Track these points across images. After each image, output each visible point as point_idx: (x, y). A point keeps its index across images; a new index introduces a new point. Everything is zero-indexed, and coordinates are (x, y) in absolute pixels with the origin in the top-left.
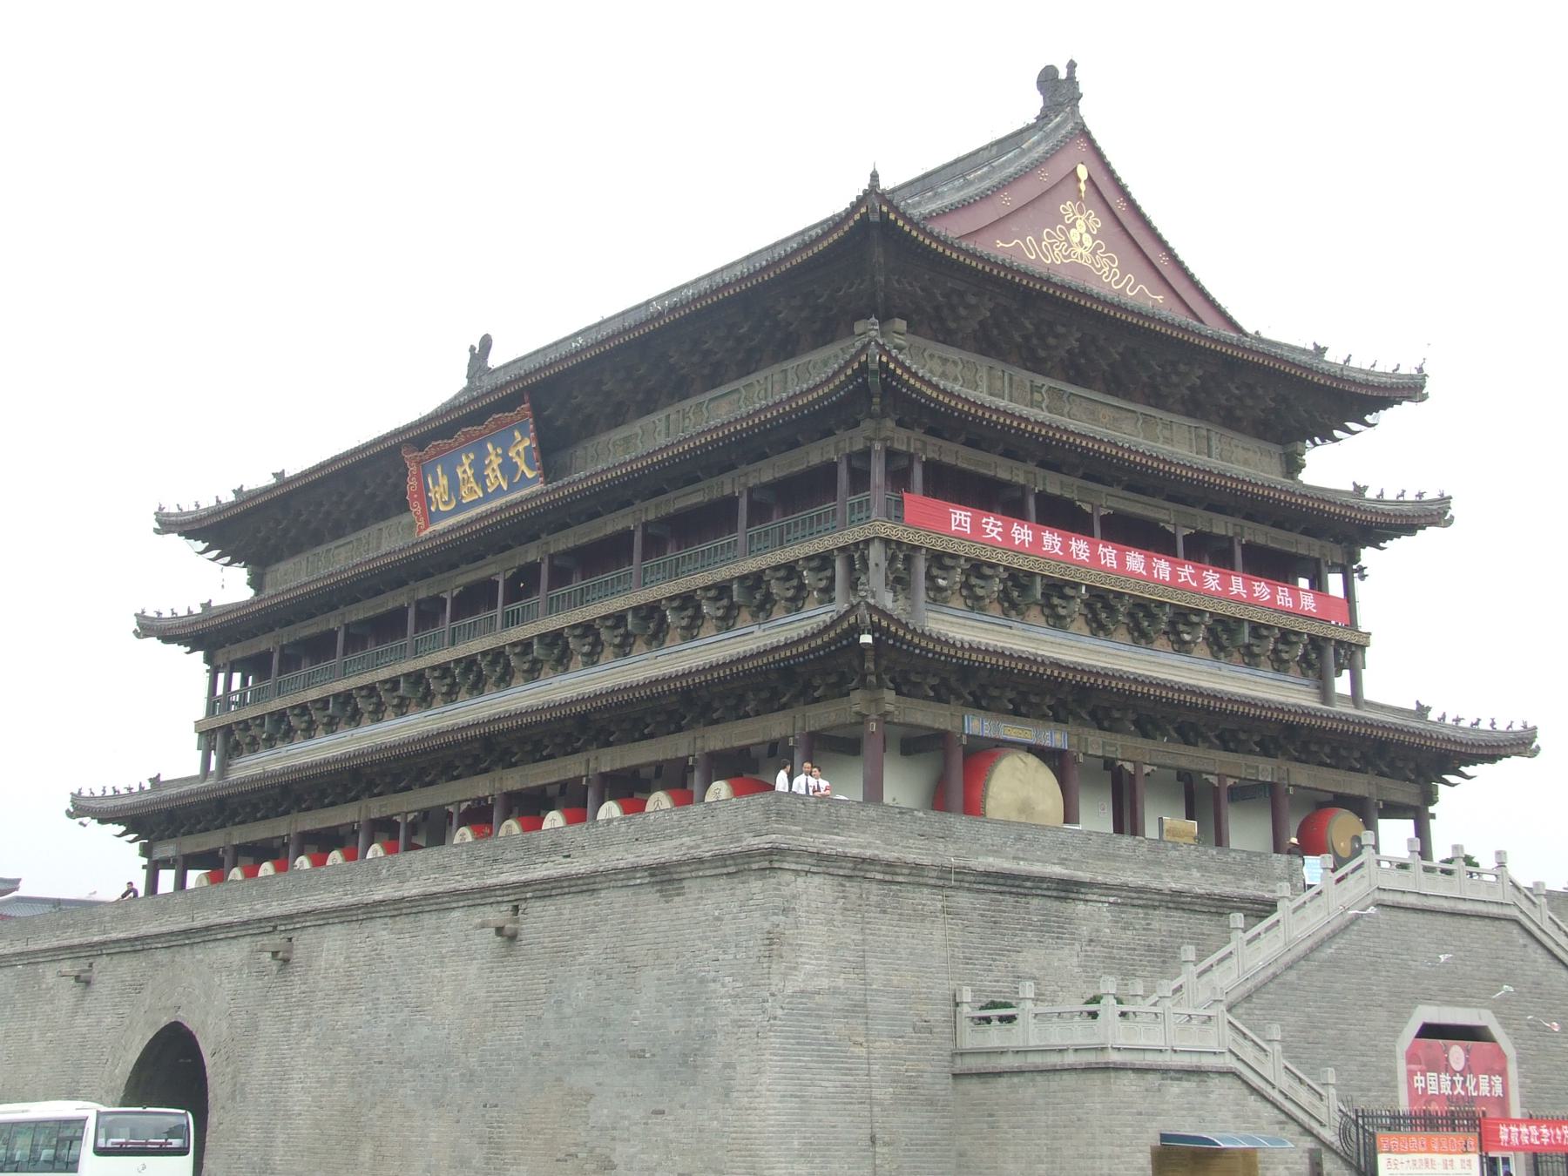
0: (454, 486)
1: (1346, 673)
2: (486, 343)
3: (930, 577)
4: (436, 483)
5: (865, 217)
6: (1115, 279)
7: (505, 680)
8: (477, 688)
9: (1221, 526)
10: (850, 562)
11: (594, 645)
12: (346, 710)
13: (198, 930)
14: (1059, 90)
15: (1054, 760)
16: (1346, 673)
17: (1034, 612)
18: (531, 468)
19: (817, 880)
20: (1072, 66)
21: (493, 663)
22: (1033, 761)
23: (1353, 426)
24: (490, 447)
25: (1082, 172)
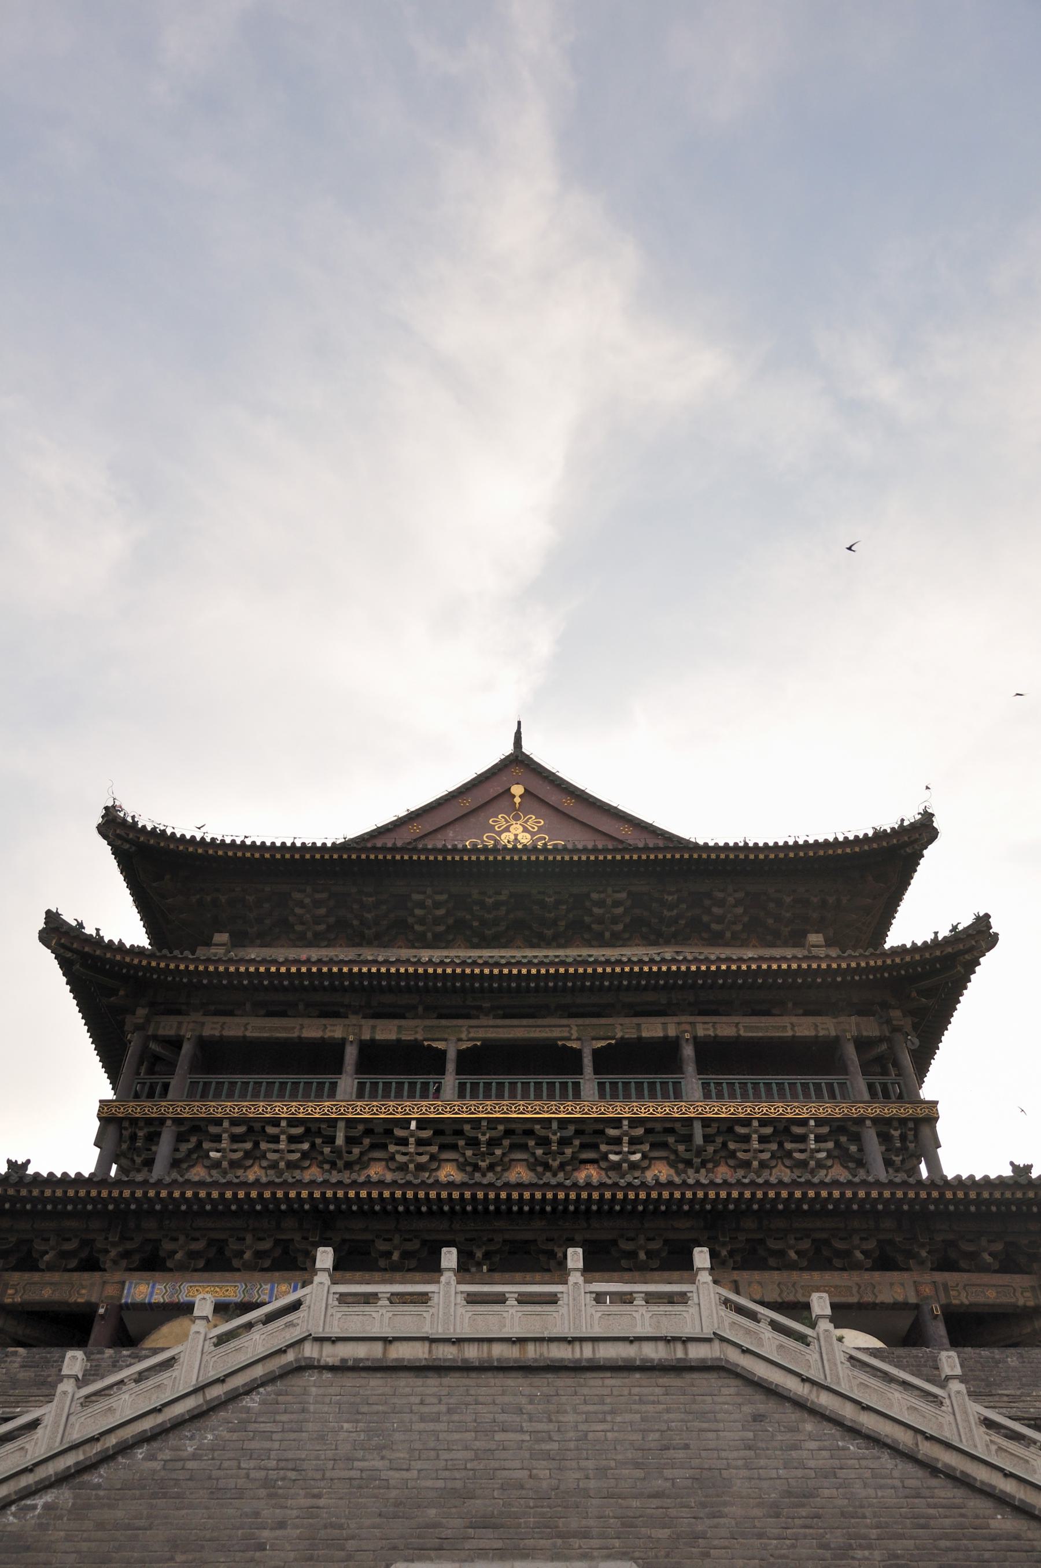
9: (653, 1029)
25: (517, 790)
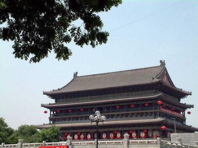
2: (77, 73)
6: (168, 84)
14: (163, 63)
20: (164, 61)
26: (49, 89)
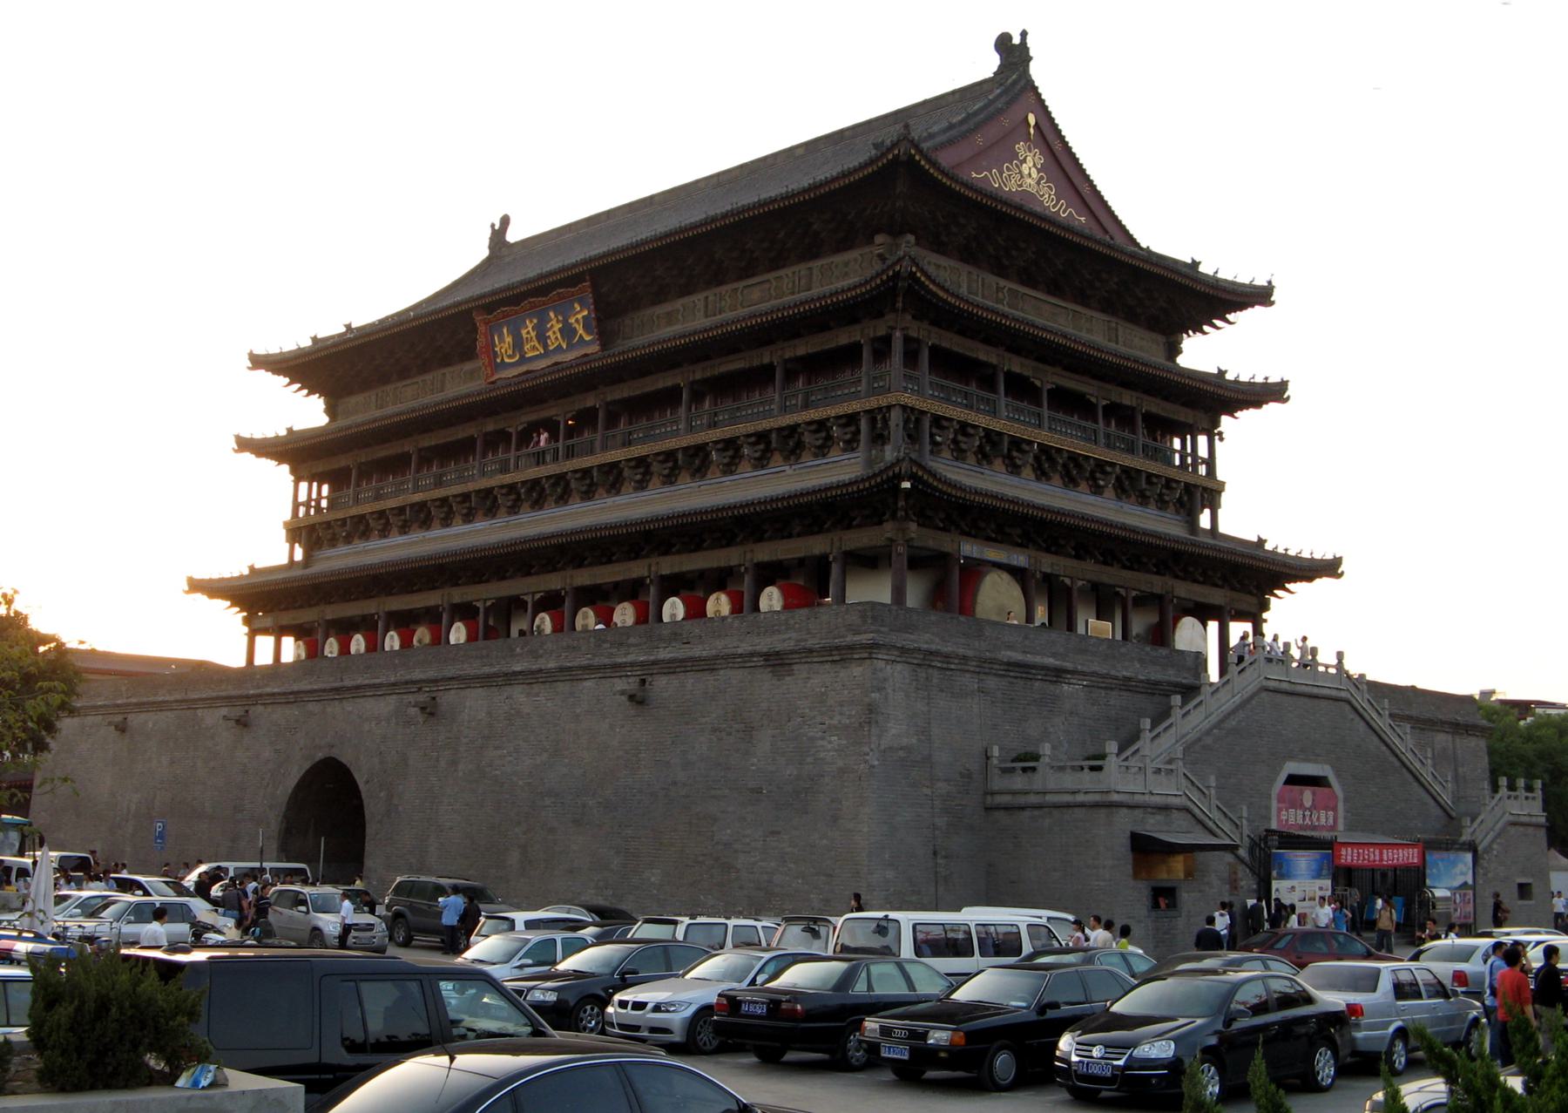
0: (518, 344)
1: (1207, 512)
2: (505, 221)
3: (932, 436)
4: (502, 340)
5: (896, 157)
7: (563, 499)
8: (538, 504)
9: (1128, 398)
10: (873, 421)
11: (644, 474)
12: (420, 516)
13: (349, 689)
14: (1013, 53)
15: (1017, 573)
16: (1207, 512)
17: (998, 462)
18: (588, 333)
19: (899, 667)
20: (1024, 34)
21: (555, 485)
22: (1006, 576)
23: (1218, 323)
24: (552, 315)
25: (1032, 119)
26: (295, 338)
